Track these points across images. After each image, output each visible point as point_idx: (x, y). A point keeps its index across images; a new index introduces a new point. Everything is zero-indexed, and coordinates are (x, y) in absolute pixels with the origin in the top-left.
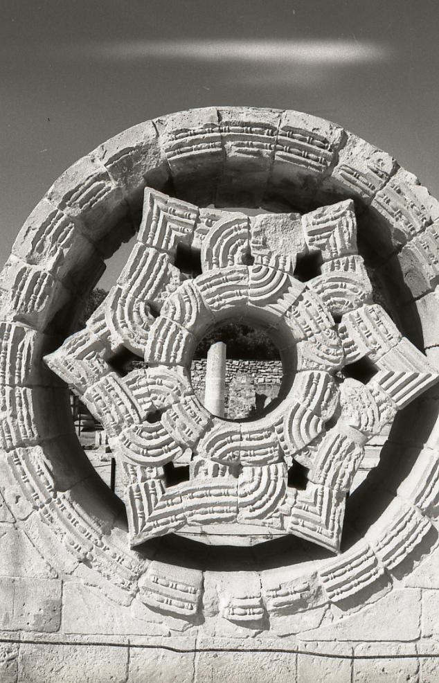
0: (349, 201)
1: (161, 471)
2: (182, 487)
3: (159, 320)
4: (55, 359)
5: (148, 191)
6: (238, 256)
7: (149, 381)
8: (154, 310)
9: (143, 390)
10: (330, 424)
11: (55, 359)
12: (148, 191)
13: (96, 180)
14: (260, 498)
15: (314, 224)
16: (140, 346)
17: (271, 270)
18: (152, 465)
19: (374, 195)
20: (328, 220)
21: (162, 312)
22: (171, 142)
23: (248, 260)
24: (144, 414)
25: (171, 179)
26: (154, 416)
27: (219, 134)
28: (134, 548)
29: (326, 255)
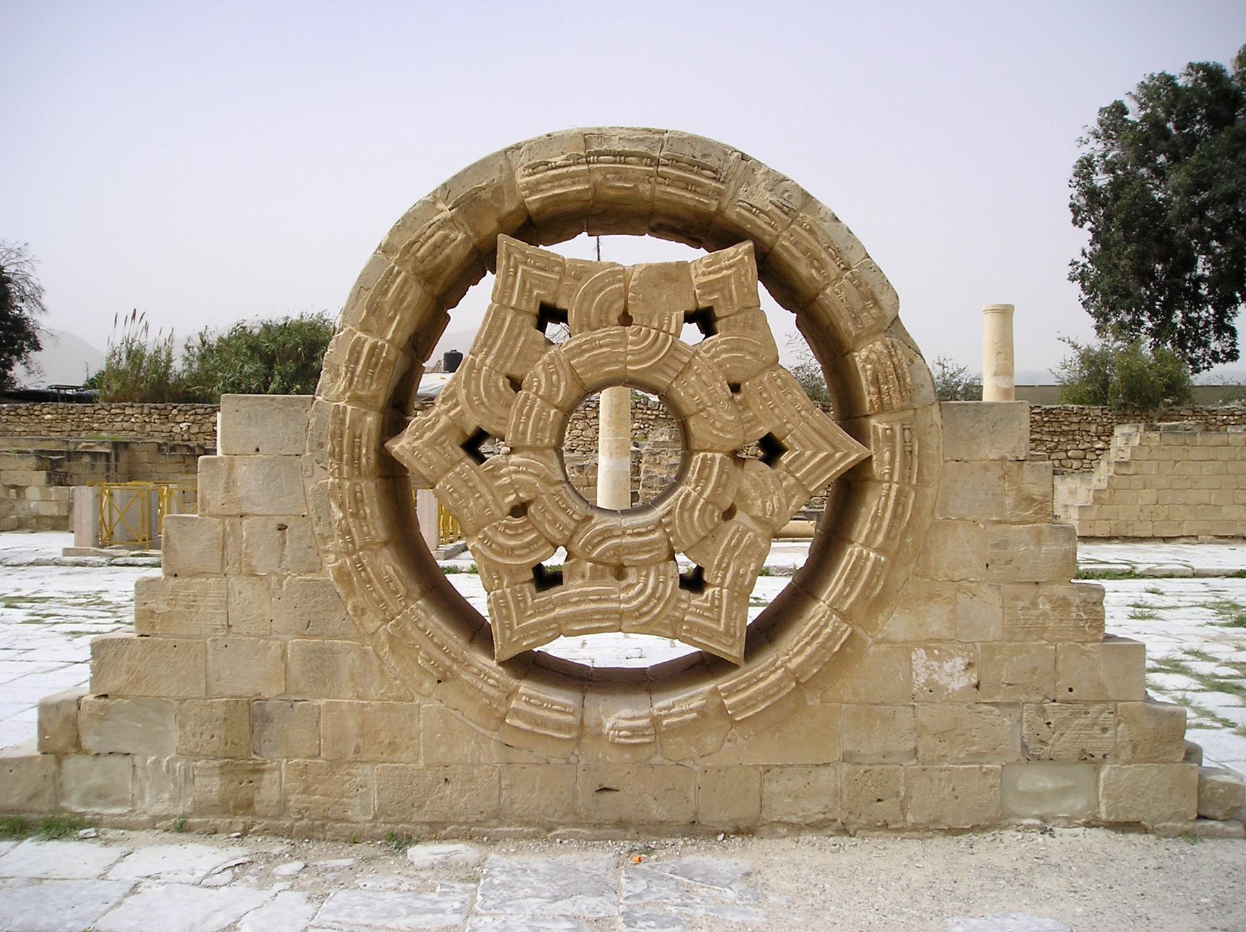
0: (747, 245)
1: (531, 576)
2: (555, 593)
3: (522, 393)
4: (400, 446)
5: (504, 240)
6: (614, 317)
7: (512, 468)
8: (516, 384)
9: (506, 480)
10: (729, 514)
11: (400, 446)
12: (504, 240)
13: (439, 228)
14: (646, 603)
15: (704, 274)
16: (498, 429)
17: (653, 332)
18: (520, 568)
19: (778, 237)
20: (721, 269)
21: (524, 384)
22: (527, 179)
23: (626, 319)
24: (507, 509)
25: (529, 218)
26: (519, 510)
27: (585, 167)
28: (501, 664)
29: (718, 314)
